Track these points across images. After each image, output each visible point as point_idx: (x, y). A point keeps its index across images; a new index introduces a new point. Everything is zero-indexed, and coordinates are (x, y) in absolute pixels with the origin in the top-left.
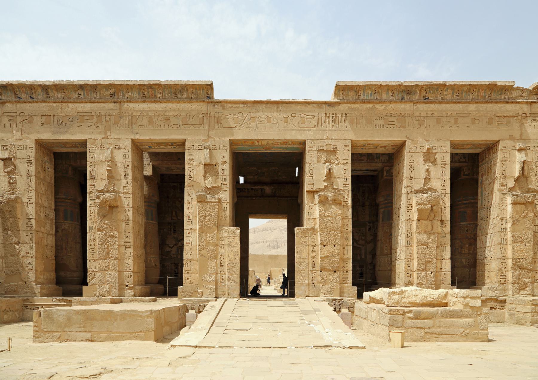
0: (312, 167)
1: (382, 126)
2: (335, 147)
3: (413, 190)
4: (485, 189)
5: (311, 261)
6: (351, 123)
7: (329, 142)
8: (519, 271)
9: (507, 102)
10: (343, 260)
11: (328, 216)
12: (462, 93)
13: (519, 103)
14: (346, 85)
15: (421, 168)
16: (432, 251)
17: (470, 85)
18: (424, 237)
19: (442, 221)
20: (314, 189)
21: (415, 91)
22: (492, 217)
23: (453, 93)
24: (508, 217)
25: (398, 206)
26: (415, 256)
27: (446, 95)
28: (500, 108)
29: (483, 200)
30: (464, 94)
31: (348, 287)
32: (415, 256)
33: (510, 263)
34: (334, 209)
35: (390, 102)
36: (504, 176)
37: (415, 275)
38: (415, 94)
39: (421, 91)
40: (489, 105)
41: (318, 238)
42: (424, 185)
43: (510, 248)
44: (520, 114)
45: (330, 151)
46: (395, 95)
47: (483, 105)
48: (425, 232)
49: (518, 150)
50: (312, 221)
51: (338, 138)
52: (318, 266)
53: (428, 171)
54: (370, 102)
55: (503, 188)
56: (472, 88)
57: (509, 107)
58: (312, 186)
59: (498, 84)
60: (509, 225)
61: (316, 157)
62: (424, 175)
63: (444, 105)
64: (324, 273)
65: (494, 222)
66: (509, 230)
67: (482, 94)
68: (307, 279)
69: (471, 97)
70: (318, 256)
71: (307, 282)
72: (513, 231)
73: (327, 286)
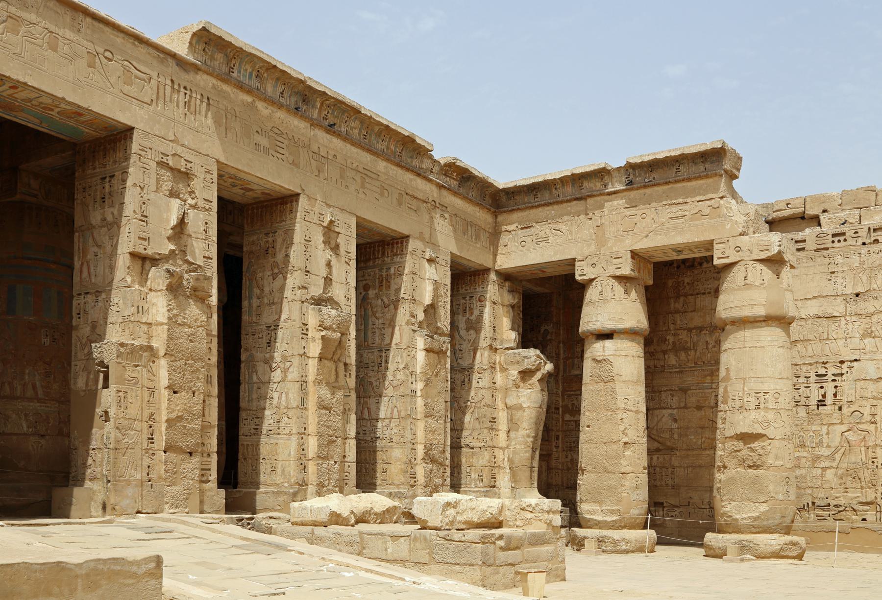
0: (146, 197)
1: (266, 151)
2: (191, 165)
3: (309, 297)
4: (374, 314)
5: (145, 425)
6: (217, 123)
7: (179, 150)
8: (430, 466)
9: (419, 175)
10: (205, 428)
11: (185, 324)
12: (370, 135)
13: (430, 181)
14: (220, 37)
15: (322, 254)
16: (336, 420)
17: (387, 126)
18: (325, 392)
19: (346, 364)
20: (150, 252)
21: (315, 101)
22: (391, 366)
23: (360, 130)
24: (418, 372)
25: (267, 318)
26: (312, 428)
27: (352, 128)
28: (411, 180)
29: (370, 334)
30: (373, 137)
31: (211, 490)
32: (312, 428)
33: (420, 450)
34: (194, 310)
35: (281, 106)
36: (414, 301)
37: (312, 468)
38: (313, 107)
39: (322, 104)
40: (400, 171)
41: (163, 373)
42: (324, 292)
43: (421, 425)
44: (430, 200)
45: (179, 171)
46: (286, 95)
47: (393, 167)
48: (328, 384)
49: (428, 260)
50: (145, 328)
51: (194, 147)
52: (161, 441)
53: (329, 264)
54: (249, 91)
55: (413, 320)
56: (387, 131)
57: (420, 183)
58: (146, 243)
59: (418, 141)
60: (420, 386)
61: (154, 176)
62: (324, 272)
63: (349, 146)
64: (172, 456)
65: (398, 377)
66: (419, 393)
67: (393, 147)
68: (139, 469)
69: (380, 146)
70: (160, 415)
71: (139, 477)
72: (425, 396)
73: (176, 488)
